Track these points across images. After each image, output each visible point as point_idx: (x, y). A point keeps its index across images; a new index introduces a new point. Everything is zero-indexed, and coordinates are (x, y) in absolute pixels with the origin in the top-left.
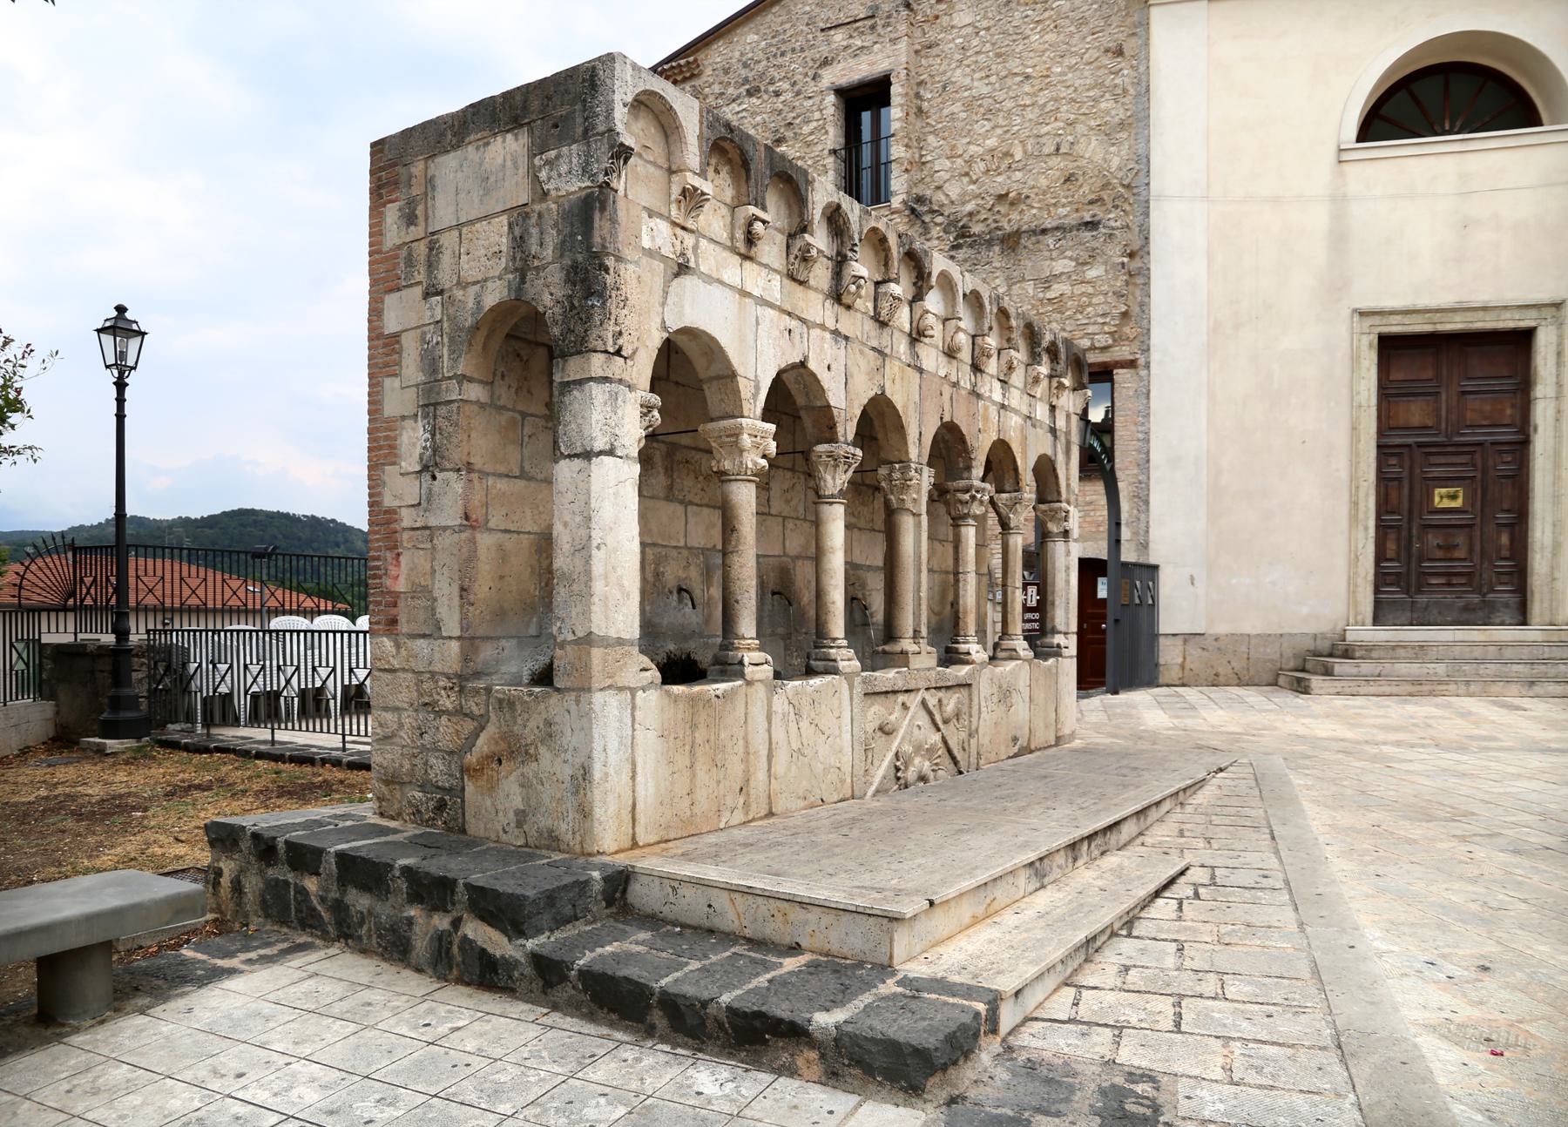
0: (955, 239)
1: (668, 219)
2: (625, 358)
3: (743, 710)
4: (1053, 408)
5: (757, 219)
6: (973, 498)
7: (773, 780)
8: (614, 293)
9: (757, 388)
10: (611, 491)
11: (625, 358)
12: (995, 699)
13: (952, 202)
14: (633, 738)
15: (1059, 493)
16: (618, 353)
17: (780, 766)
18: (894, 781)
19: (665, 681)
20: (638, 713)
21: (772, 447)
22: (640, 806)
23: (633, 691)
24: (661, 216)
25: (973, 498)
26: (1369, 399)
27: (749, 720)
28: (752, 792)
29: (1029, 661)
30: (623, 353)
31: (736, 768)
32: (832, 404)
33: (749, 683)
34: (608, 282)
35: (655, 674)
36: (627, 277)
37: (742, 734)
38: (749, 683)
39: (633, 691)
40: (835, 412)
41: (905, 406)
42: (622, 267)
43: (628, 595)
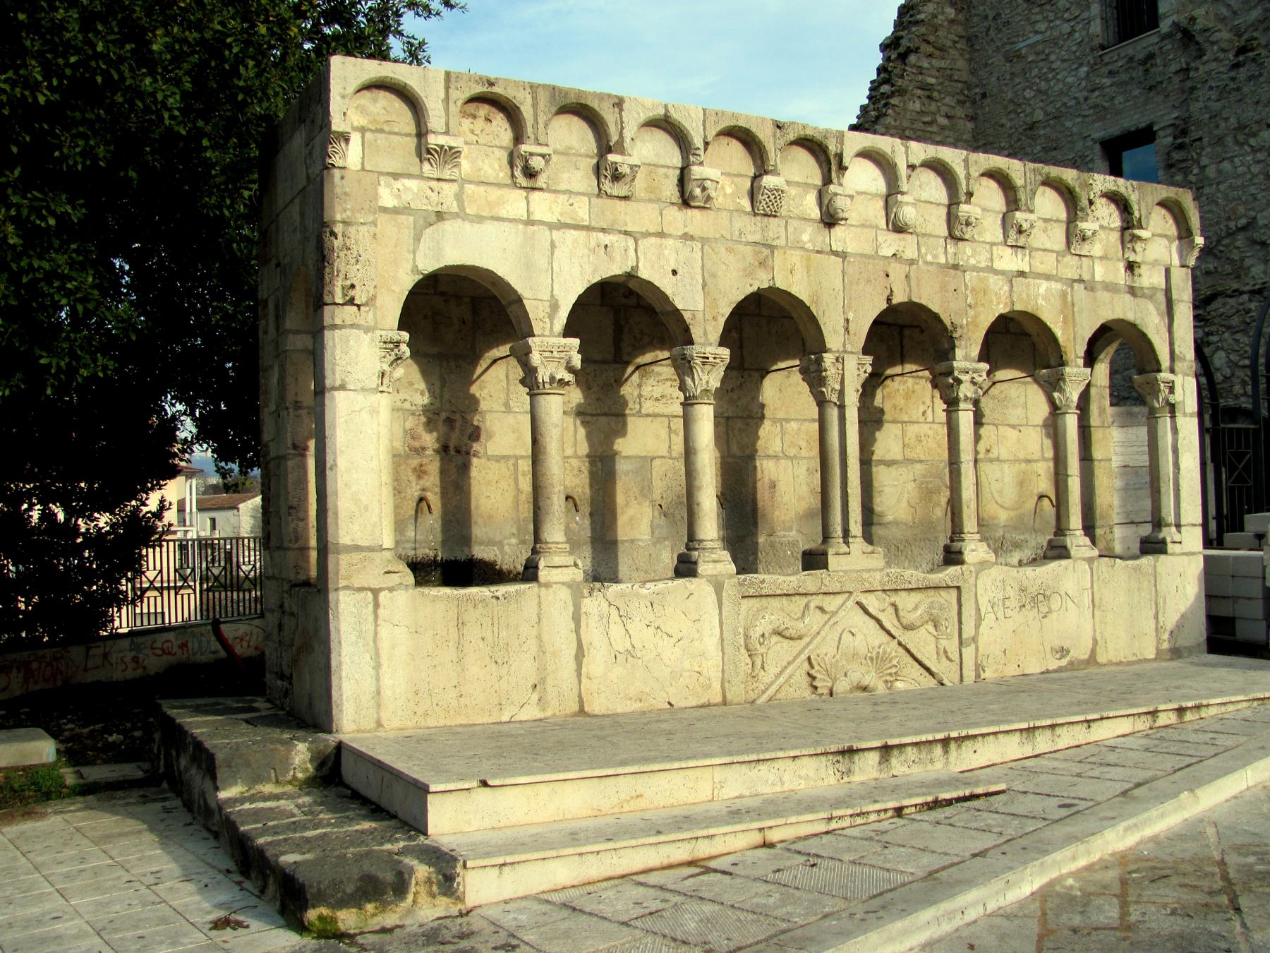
0: (1237, 55)
1: (421, 177)
2: (359, 306)
3: (534, 610)
4: (1131, 267)
5: (531, 154)
6: (959, 382)
7: (584, 679)
8: (342, 254)
9: (555, 306)
10: (342, 420)
11: (359, 306)
12: (1013, 603)
13: (1235, 13)
14: (376, 633)
15: (1158, 362)
16: (351, 302)
17: (596, 664)
18: (809, 690)
19: (418, 583)
20: (381, 611)
21: (577, 361)
22: (387, 693)
23: (376, 592)
24: (409, 176)
25: (959, 382)
26: (1117, 252)
27: (544, 621)
28: (549, 689)
29: (1090, 561)
30: (356, 302)
31: (524, 668)
32: (680, 307)
33: (548, 585)
34: (336, 245)
35: (410, 578)
36: (360, 237)
37: (534, 632)
38: (548, 585)
39: (376, 592)
40: (687, 316)
41: (816, 297)
42: (352, 230)
43: (366, 508)
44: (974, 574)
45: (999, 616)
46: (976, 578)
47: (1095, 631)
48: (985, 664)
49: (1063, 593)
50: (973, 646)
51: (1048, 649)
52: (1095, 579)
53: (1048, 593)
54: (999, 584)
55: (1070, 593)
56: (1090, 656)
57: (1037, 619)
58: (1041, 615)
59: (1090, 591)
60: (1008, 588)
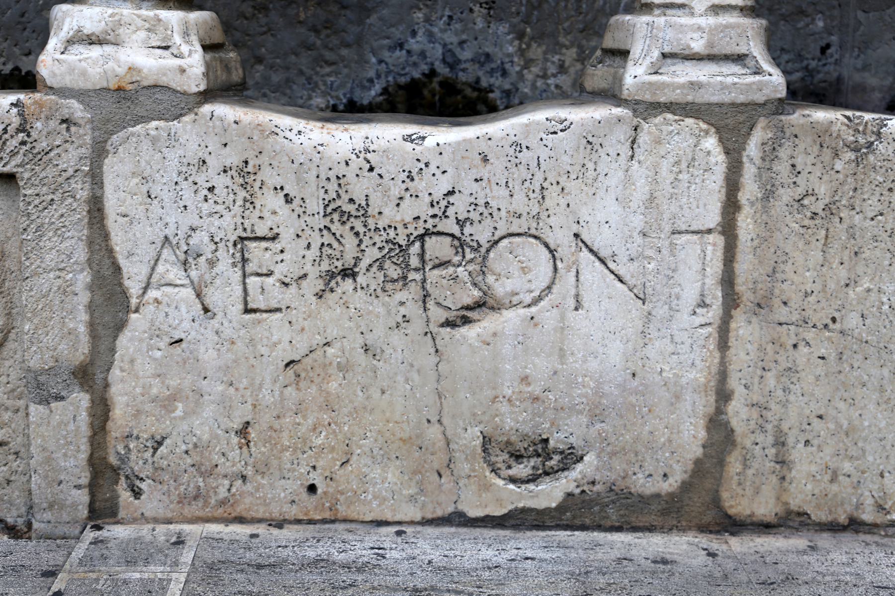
44: (86, 135)
45: (213, 297)
46: (99, 152)
47: (723, 395)
48: (136, 464)
49: (561, 238)
50: (81, 400)
51: (472, 437)
52: (749, 190)
53: (482, 233)
54: (220, 182)
55: (601, 240)
56: (686, 487)
57: (417, 326)
58: (438, 315)
59: (716, 243)
60: (273, 201)
